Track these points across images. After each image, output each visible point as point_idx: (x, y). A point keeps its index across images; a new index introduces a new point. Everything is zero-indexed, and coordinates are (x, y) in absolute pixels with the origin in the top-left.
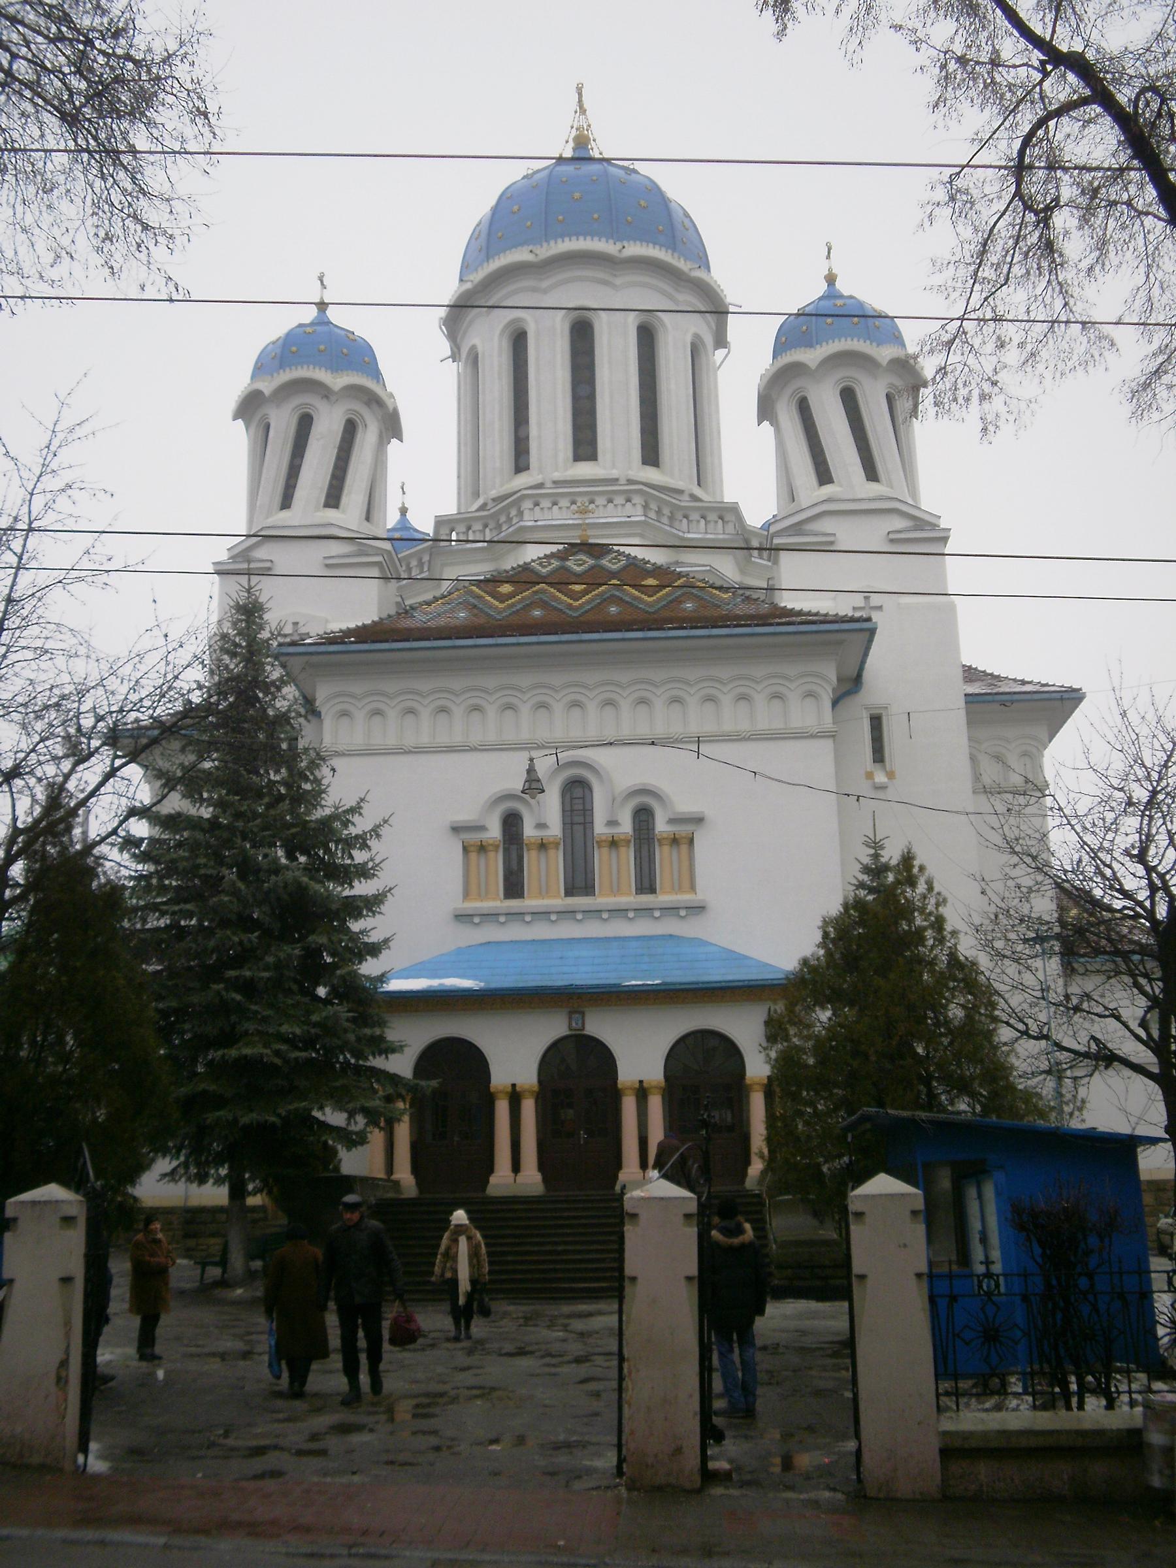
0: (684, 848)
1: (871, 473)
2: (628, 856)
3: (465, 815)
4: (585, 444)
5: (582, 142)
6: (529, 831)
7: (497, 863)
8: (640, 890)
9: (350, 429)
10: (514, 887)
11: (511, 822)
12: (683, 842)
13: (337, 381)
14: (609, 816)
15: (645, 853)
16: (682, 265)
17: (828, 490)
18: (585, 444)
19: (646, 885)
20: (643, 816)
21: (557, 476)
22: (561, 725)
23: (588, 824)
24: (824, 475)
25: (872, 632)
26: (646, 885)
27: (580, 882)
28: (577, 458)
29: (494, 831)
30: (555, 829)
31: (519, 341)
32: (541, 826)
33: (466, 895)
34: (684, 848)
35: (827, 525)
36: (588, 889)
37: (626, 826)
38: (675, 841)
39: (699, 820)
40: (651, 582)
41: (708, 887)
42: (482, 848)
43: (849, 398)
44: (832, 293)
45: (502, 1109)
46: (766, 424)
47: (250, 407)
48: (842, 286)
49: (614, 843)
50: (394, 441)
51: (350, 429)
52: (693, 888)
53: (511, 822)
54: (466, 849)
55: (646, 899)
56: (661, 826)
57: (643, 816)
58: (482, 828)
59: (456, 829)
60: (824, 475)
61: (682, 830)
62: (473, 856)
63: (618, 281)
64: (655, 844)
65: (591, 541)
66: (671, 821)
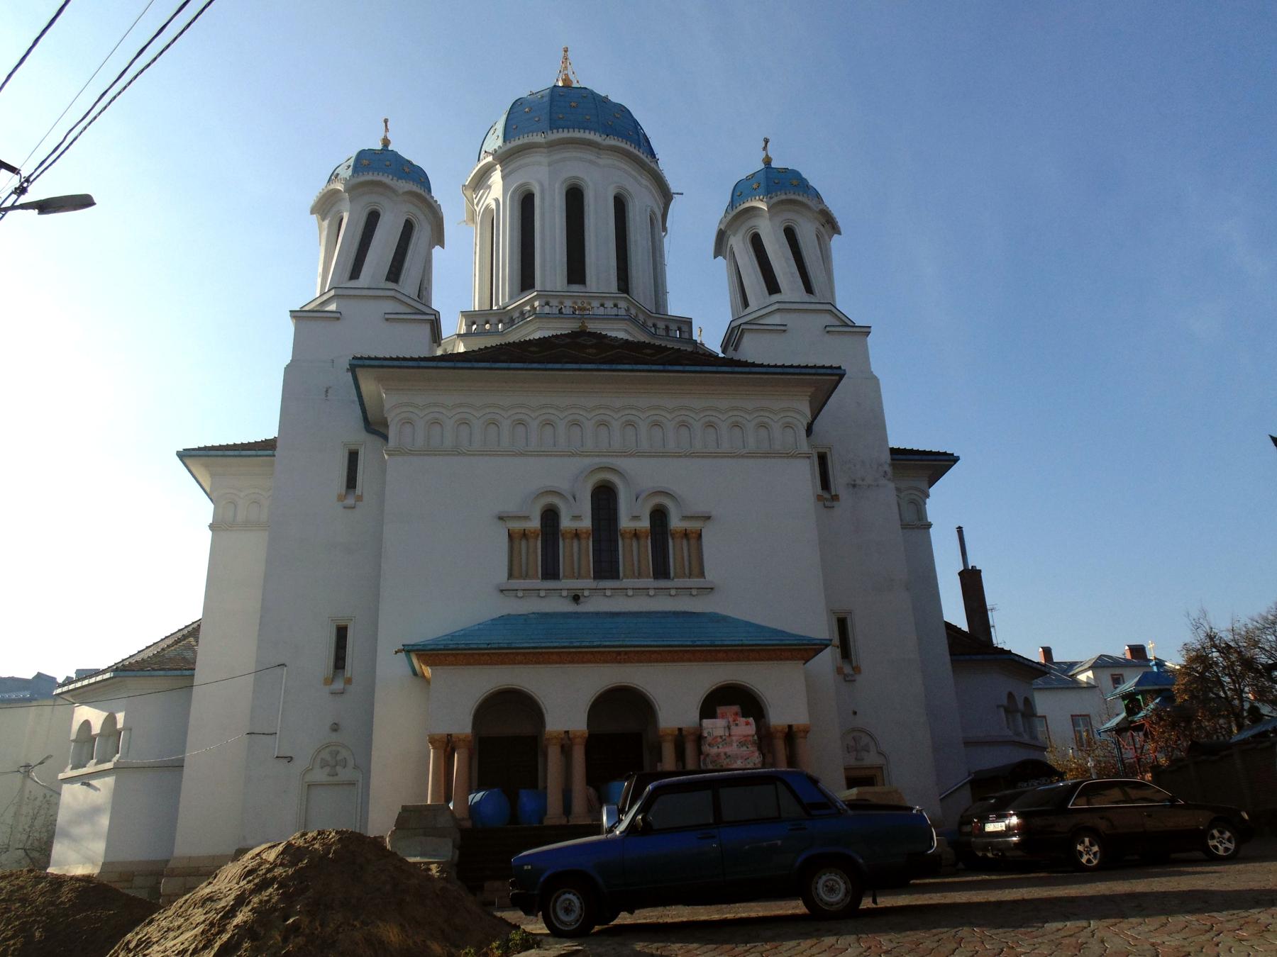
0: (693, 542)
1: (809, 289)
3: (511, 507)
4: (576, 272)
6: (566, 523)
9: (408, 228)
10: (550, 572)
11: (550, 516)
13: (404, 186)
16: (647, 160)
17: (776, 297)
18: (576, 272)
19: (661, 571)
20: (659, 515)
24: (773, 286)
25: (842, 376)
27: (606, 567)
29: (535, 524)
30: (586, 523)
33: (511, 576)
34: (693, 542)
35: (776, 319)
36: (615, 575)
37: (645, 524)
38: (686, 534)
40: (648, 351)
41: (713, 572)
42: (525, 535)
45: (554, 755)
46: (720, 258)
47: (325, 206)
50: (437, 248)
51: (408, 228)
52: (702, 574)
53: (550, 516)
54: (511, 536)
55: (662, 583)
56: (675, 523)
57: (659, 515)
58: (526, 518)
59: (501, 518)
60: (773, 286)
63: (601, 162)
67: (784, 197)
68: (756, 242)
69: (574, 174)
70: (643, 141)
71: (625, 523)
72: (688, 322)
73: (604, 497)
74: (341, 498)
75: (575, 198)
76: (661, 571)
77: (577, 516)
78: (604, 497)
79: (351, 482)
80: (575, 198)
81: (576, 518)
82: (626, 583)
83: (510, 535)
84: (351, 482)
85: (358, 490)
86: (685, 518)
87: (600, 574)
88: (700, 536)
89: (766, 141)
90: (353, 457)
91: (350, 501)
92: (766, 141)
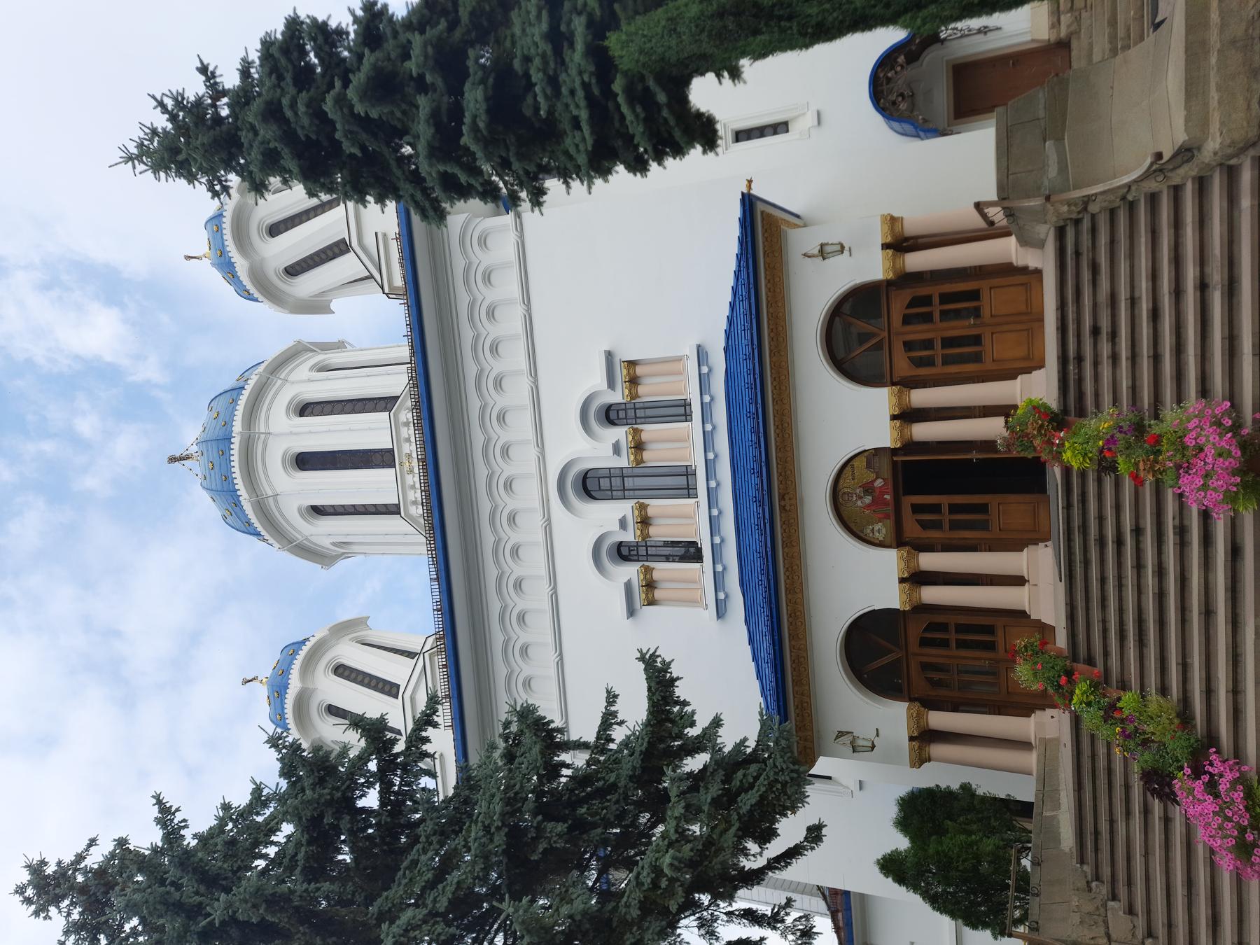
0: (639, 370)
2: (650, 431)
6: (630, 536)
7: (662, 570)
8: (687, 417)
12: (632, 374)
14: (603, 450)
15: (649, 412)
19: (680, 411)
22: (527, 497)
23: (622, 473)
26: (680, 411)
29: (631, 571)
30: (625, 508)
32: (623, 524)
34: (639, 370)
37: (620, 434)
38: (633, 381)
49: (639, 447)
52: (678, 359)
53: (623, 553)
56: (618, 396)
61: (621, 373)
62: (658, 594)
64: (627, 405)
66: (611, 384)
75: (305, 461)
80: (305, 461)
83: (649, 604)
88: (632, 364)
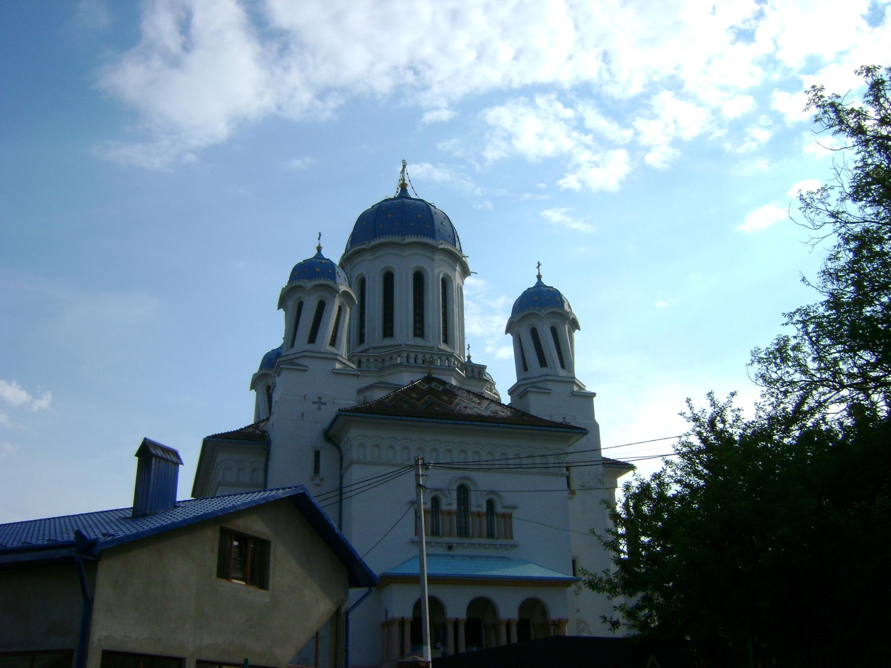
4: (419, 330)
5: (403, 187)
6: (444, 507)
12: (507, 517)
20: (490, 504)
21: (408, 343)
24: (543, 363)
28: (415, 335)
30: (454, 507)
31: (388, 279)
37: (484, 509)
39: (515, 508)
43: (554, 330)
44: (539, 283)
48: (546, 282)
52: (512, 538)
53: (435, 501)
55: (492, 541)
56: (499, 509)
57: (490, 504)
60: (543, 363)
61: (508, 511)
65: (433, 376)
66: (504, 507)
67: (552, 310)
68: (534, 333)
69: (421, 265)
70: (457, 244)
71: (473, 509)
72: (484, 367)
73: (463, 492)
74: (312, 479)
75: (419, 278)
76: (491, 535)
77: (450, 503)
78: (463, 492)
79: (317, 469)
81: (450, 504)
82: (475, 540)
84: (317, 469)
85: (321, 475)
86: (504, 507)
87: (460, 534)
89: (539, 265)
90: (317, 454)
91: (317, 481)
92: (539, 265)
